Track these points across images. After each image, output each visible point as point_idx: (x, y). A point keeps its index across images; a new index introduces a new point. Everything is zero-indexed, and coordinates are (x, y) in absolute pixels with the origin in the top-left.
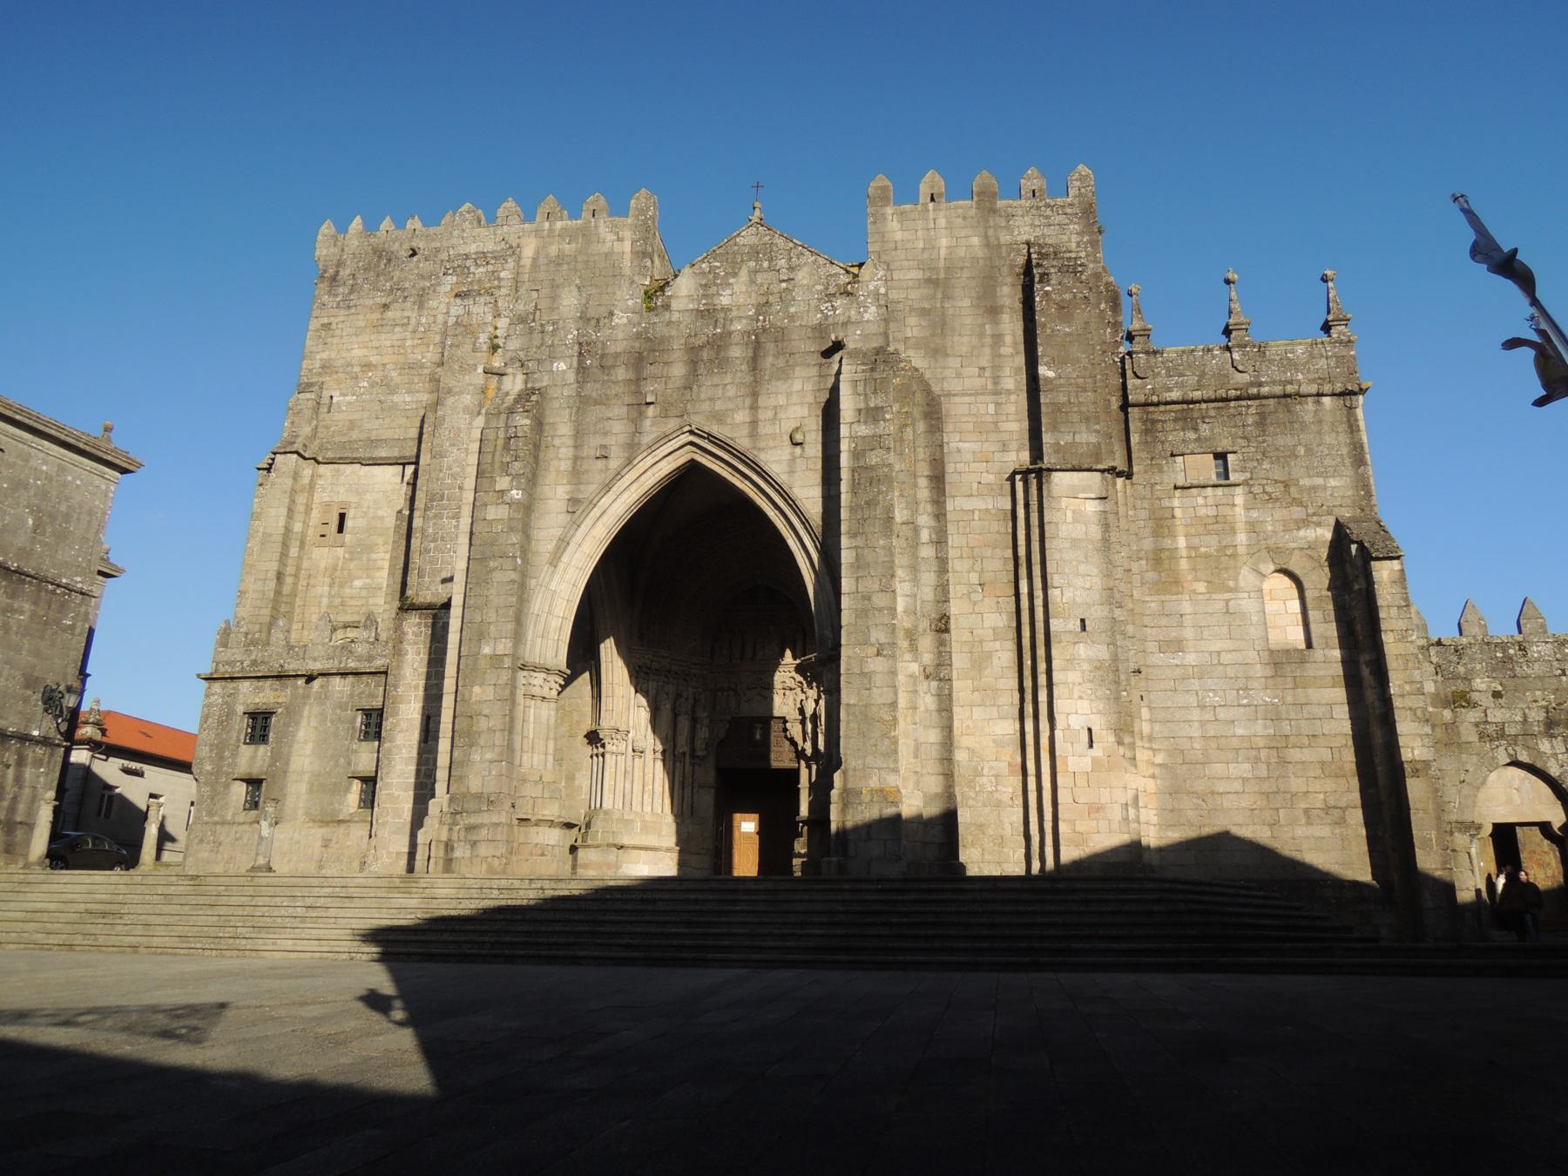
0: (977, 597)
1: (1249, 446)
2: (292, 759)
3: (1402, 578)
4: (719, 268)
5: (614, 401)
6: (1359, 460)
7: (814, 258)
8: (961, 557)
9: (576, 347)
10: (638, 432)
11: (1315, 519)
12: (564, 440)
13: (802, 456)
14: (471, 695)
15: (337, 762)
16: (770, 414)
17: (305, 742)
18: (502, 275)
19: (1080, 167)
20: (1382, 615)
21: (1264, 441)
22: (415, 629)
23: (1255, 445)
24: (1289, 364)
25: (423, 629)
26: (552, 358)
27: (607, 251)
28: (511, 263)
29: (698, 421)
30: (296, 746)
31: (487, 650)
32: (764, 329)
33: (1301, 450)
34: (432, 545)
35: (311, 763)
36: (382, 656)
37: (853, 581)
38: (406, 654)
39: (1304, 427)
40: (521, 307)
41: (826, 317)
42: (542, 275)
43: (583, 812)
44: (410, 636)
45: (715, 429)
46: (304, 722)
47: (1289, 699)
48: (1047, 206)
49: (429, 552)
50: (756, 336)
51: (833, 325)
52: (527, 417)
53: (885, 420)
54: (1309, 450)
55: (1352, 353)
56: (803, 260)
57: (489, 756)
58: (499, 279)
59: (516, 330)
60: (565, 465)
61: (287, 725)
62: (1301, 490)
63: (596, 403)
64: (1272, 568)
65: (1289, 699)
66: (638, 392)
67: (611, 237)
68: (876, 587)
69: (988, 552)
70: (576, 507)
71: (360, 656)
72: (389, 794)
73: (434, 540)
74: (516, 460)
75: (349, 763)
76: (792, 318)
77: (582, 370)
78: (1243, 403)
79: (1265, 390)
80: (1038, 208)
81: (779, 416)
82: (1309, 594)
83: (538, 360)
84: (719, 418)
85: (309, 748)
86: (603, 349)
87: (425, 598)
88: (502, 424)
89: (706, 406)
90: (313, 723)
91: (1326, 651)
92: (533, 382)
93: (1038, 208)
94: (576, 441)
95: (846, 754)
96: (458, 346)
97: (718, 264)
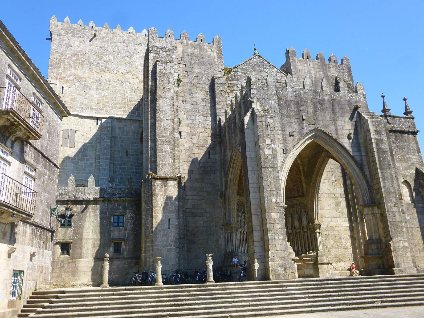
0: (335, 184)
2: (84, 234)
6: (419, 152)
9: (276, 96)
10: (301, 128)
11: (411, 167)
14: (271, 216)
15: (104, 235)
16: (341, 127)
17: (89, 227)
18: (173, 57)
21: (397, 144)
22: (160, 186)
25: (163, 186)
26: (269, 99)
28: (175, 53)
29: (320, 127)
30: (85, 229)
31: (274, 200)
32: (334, 100)
33: (406, 147)
35: (92, 235)
36: (119, 194)
39: (406, 141)
40: (254, 79)
42: (186, 59)
43: (223, 253)
45: (325, 130)
46: (88, 219)
51: (353, 101)
52: (272, 119)
53: (383, 134)
54: (407, 147)
56: (273, 70)
58: (172, 58)
60: (280, 137)
61: (80, 220)
62: (407, 158)
65: (411, 217)
66: (299, 115)
67: (209, 50)
69: (336, 170)
70: (285, 152)
71: (109, 193)
72: (157, 249)
73: (162, 152)
74: (271, 134)
75: (110, 235)
76: (341, 98)
79: (397, 129)
80: (336, 66)
84: (326, 126)
85: (91, 230)
86: (286, 99)
88: (264, 120)
90: (92, 219)
93: (336, 66)
95: (392, 237)
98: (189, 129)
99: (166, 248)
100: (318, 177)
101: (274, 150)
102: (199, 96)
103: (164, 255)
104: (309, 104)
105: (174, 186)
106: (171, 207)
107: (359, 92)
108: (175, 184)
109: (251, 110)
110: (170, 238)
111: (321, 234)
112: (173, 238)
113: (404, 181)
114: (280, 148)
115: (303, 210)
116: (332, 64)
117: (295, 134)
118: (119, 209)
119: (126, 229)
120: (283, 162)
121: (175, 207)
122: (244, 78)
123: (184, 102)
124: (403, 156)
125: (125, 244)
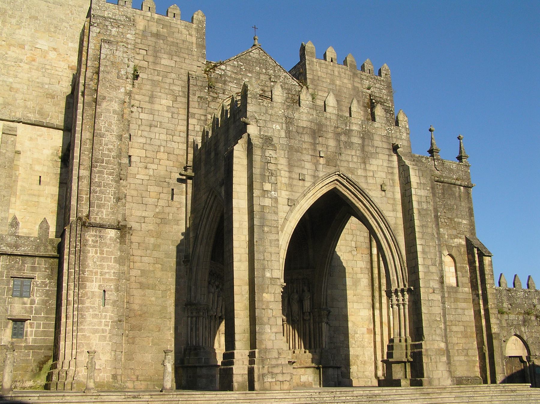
0: (355, 253)
1: (440, 202)
3: (491, 265)
4: (242, 66)
5: (304, 152)
6: (471, 214)
7: (285, 74)
8: (348, 234)
9: (284, 119)
10: (316, 170)
11: (459, 235)
12: (282, 167)
13: (385, 196)
16: (371, 174)
18: (129, 36)
19: (385, 65)
20: (486, 277)
21: (444, 201)
22: (93, 238)
23: (442, 201)
24: (451, 170)
27: (183, 39)
29: (343, 170)
34: (98, 189)
37: (422, 259)
38: (89, 252)
41: (389, 133)
43: (183, 347)
44: (90, 242)
45: (350, 176)
47: (453, 307)
48: (374, 78)
49: (96, 192)
50: (362, 134)
55: (469, 171)
57: (274, 330)
59: (252, 101)
60: (285, 180)
62: (455, 222)
63: (297, 151)
64: (448, 254)
65: (453, 307)
67: (185, 31)
68: (430, 263)
69: (358, 233)
70: (292, 203)
73: (99, 186)
75: (7, 310)
77: (288, 132)
78: (438, 183)
81: (375, 176)
82: (458, 265)
83: (265, 121)
87: (95, 220)
89: (345, 164)
91: (463, 288)
92: (265, 131)
93: (372, 78)
94: (289, 169)
96: (108, 73)
97: (242, 64)
98: (143, 153)
99: (98, 335)
100: (333, 242)
101: (276, 200)
102: (164, 102)
103: (93, 346)
104: (330, 135)
105: (115, 240)
106: (108, 273)
107: (402, 124)
108: (117, 238)
109: (245, 136)
110: (103, 320)
111: (329, 325)
112: (108, 320)
113: (448, 255)
114: (283, 195)
115: (306, 288)
116: (366, 74)
117: (308, 178)
118: (24, 270)
119: (33, 302)
120: (286, 219)
121: (114, 273)
122: (235, 81)
123: (140, 110)
124: (451, 219)
125: (31, 324)
